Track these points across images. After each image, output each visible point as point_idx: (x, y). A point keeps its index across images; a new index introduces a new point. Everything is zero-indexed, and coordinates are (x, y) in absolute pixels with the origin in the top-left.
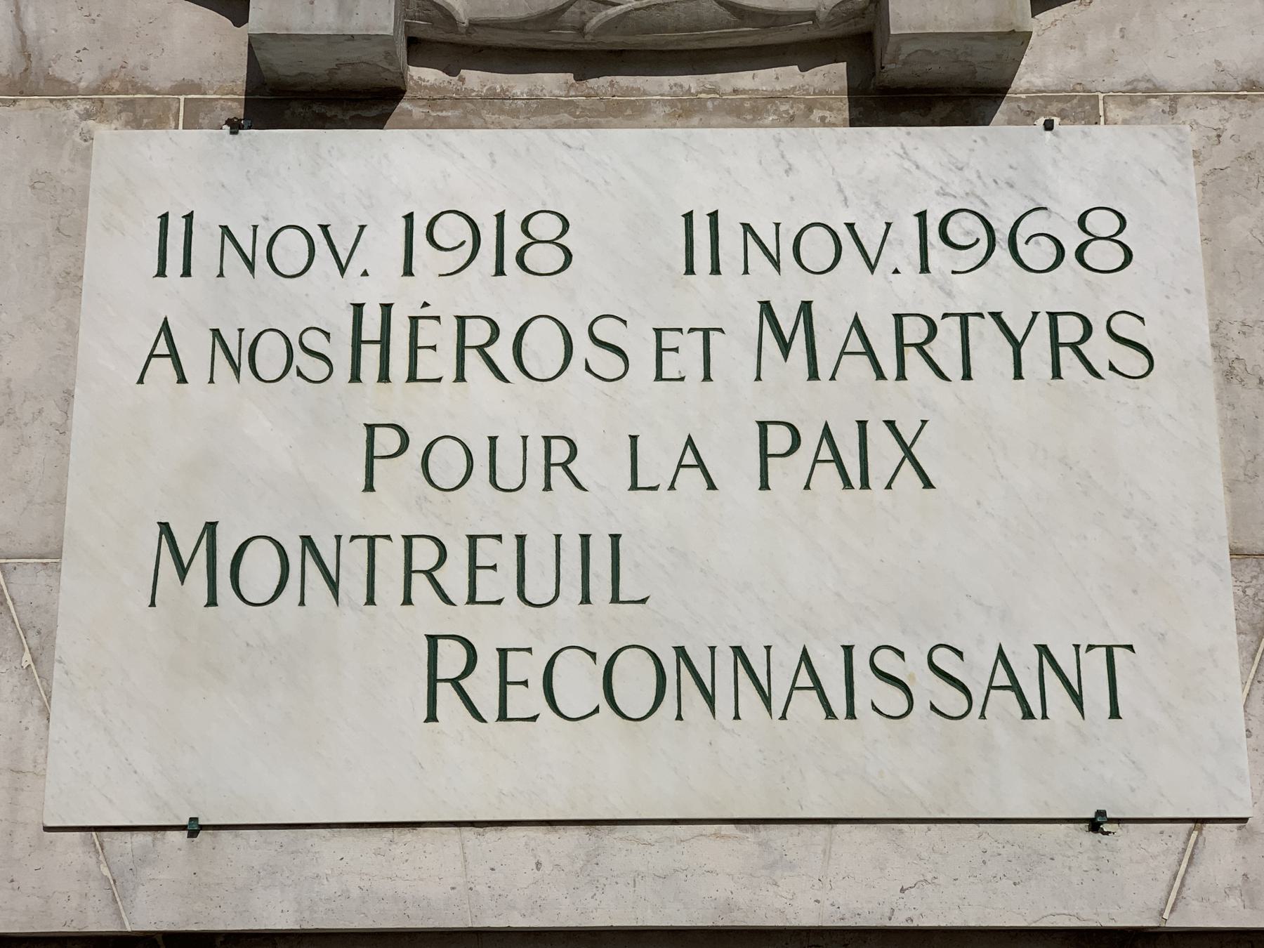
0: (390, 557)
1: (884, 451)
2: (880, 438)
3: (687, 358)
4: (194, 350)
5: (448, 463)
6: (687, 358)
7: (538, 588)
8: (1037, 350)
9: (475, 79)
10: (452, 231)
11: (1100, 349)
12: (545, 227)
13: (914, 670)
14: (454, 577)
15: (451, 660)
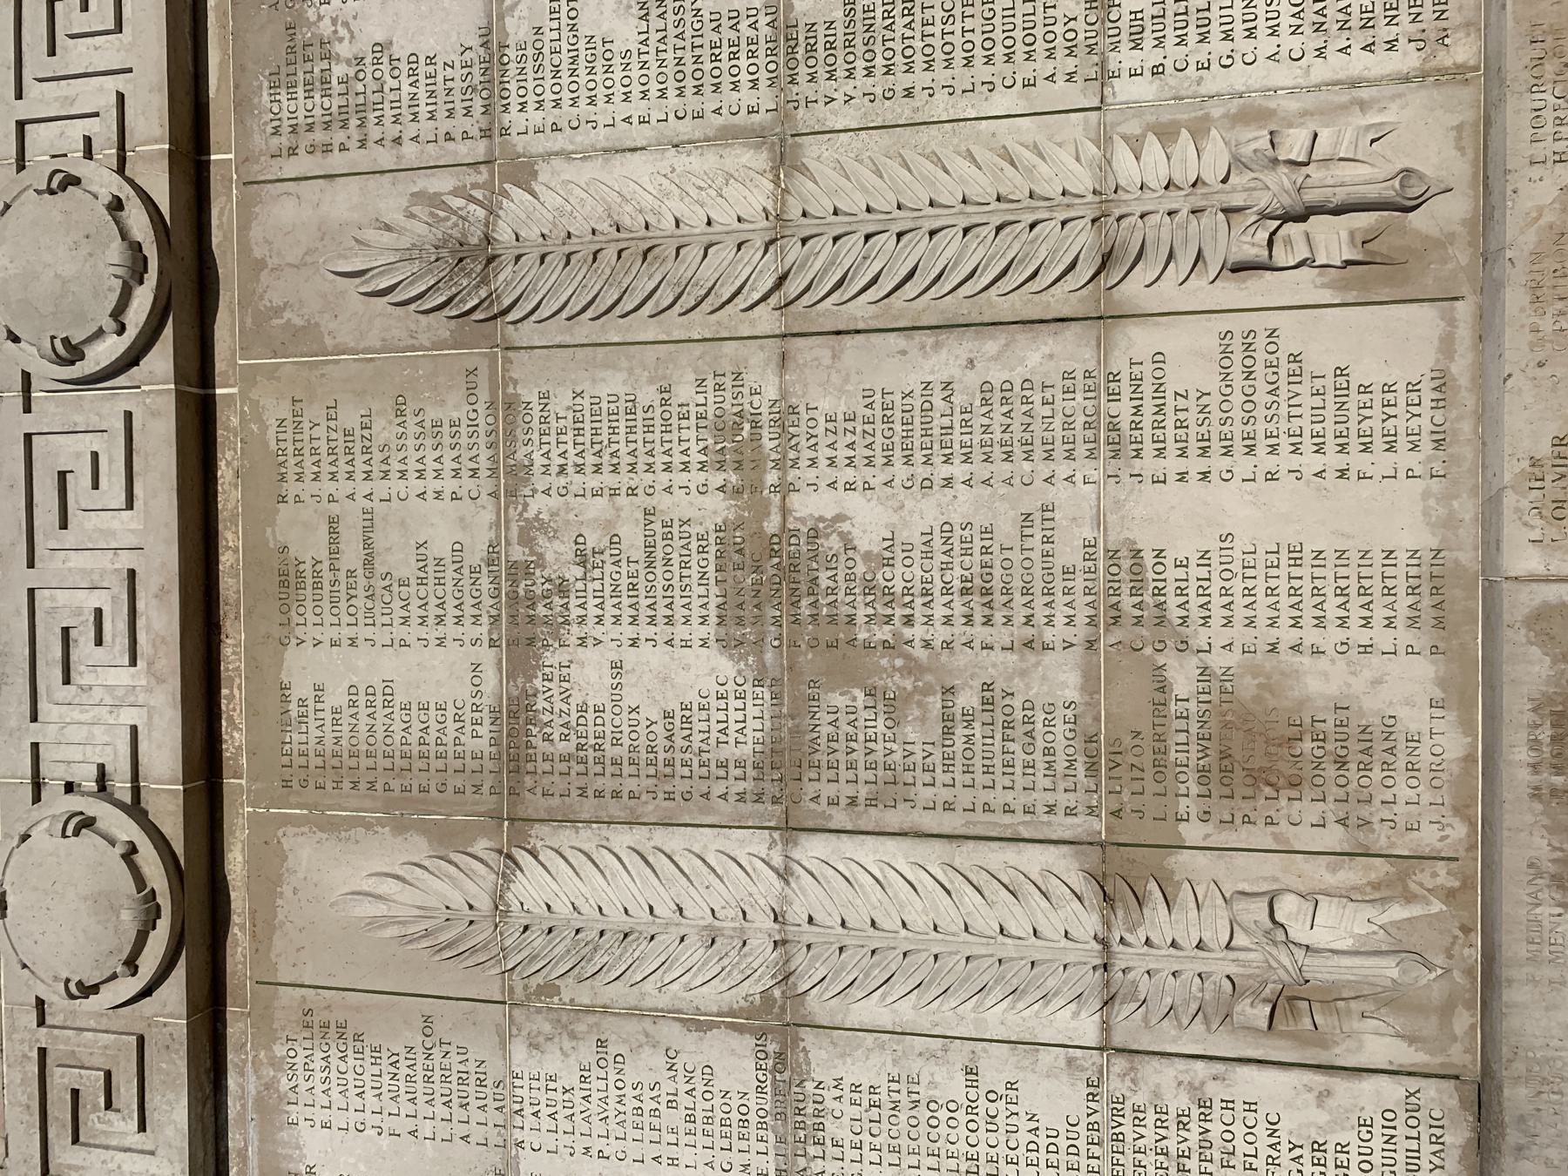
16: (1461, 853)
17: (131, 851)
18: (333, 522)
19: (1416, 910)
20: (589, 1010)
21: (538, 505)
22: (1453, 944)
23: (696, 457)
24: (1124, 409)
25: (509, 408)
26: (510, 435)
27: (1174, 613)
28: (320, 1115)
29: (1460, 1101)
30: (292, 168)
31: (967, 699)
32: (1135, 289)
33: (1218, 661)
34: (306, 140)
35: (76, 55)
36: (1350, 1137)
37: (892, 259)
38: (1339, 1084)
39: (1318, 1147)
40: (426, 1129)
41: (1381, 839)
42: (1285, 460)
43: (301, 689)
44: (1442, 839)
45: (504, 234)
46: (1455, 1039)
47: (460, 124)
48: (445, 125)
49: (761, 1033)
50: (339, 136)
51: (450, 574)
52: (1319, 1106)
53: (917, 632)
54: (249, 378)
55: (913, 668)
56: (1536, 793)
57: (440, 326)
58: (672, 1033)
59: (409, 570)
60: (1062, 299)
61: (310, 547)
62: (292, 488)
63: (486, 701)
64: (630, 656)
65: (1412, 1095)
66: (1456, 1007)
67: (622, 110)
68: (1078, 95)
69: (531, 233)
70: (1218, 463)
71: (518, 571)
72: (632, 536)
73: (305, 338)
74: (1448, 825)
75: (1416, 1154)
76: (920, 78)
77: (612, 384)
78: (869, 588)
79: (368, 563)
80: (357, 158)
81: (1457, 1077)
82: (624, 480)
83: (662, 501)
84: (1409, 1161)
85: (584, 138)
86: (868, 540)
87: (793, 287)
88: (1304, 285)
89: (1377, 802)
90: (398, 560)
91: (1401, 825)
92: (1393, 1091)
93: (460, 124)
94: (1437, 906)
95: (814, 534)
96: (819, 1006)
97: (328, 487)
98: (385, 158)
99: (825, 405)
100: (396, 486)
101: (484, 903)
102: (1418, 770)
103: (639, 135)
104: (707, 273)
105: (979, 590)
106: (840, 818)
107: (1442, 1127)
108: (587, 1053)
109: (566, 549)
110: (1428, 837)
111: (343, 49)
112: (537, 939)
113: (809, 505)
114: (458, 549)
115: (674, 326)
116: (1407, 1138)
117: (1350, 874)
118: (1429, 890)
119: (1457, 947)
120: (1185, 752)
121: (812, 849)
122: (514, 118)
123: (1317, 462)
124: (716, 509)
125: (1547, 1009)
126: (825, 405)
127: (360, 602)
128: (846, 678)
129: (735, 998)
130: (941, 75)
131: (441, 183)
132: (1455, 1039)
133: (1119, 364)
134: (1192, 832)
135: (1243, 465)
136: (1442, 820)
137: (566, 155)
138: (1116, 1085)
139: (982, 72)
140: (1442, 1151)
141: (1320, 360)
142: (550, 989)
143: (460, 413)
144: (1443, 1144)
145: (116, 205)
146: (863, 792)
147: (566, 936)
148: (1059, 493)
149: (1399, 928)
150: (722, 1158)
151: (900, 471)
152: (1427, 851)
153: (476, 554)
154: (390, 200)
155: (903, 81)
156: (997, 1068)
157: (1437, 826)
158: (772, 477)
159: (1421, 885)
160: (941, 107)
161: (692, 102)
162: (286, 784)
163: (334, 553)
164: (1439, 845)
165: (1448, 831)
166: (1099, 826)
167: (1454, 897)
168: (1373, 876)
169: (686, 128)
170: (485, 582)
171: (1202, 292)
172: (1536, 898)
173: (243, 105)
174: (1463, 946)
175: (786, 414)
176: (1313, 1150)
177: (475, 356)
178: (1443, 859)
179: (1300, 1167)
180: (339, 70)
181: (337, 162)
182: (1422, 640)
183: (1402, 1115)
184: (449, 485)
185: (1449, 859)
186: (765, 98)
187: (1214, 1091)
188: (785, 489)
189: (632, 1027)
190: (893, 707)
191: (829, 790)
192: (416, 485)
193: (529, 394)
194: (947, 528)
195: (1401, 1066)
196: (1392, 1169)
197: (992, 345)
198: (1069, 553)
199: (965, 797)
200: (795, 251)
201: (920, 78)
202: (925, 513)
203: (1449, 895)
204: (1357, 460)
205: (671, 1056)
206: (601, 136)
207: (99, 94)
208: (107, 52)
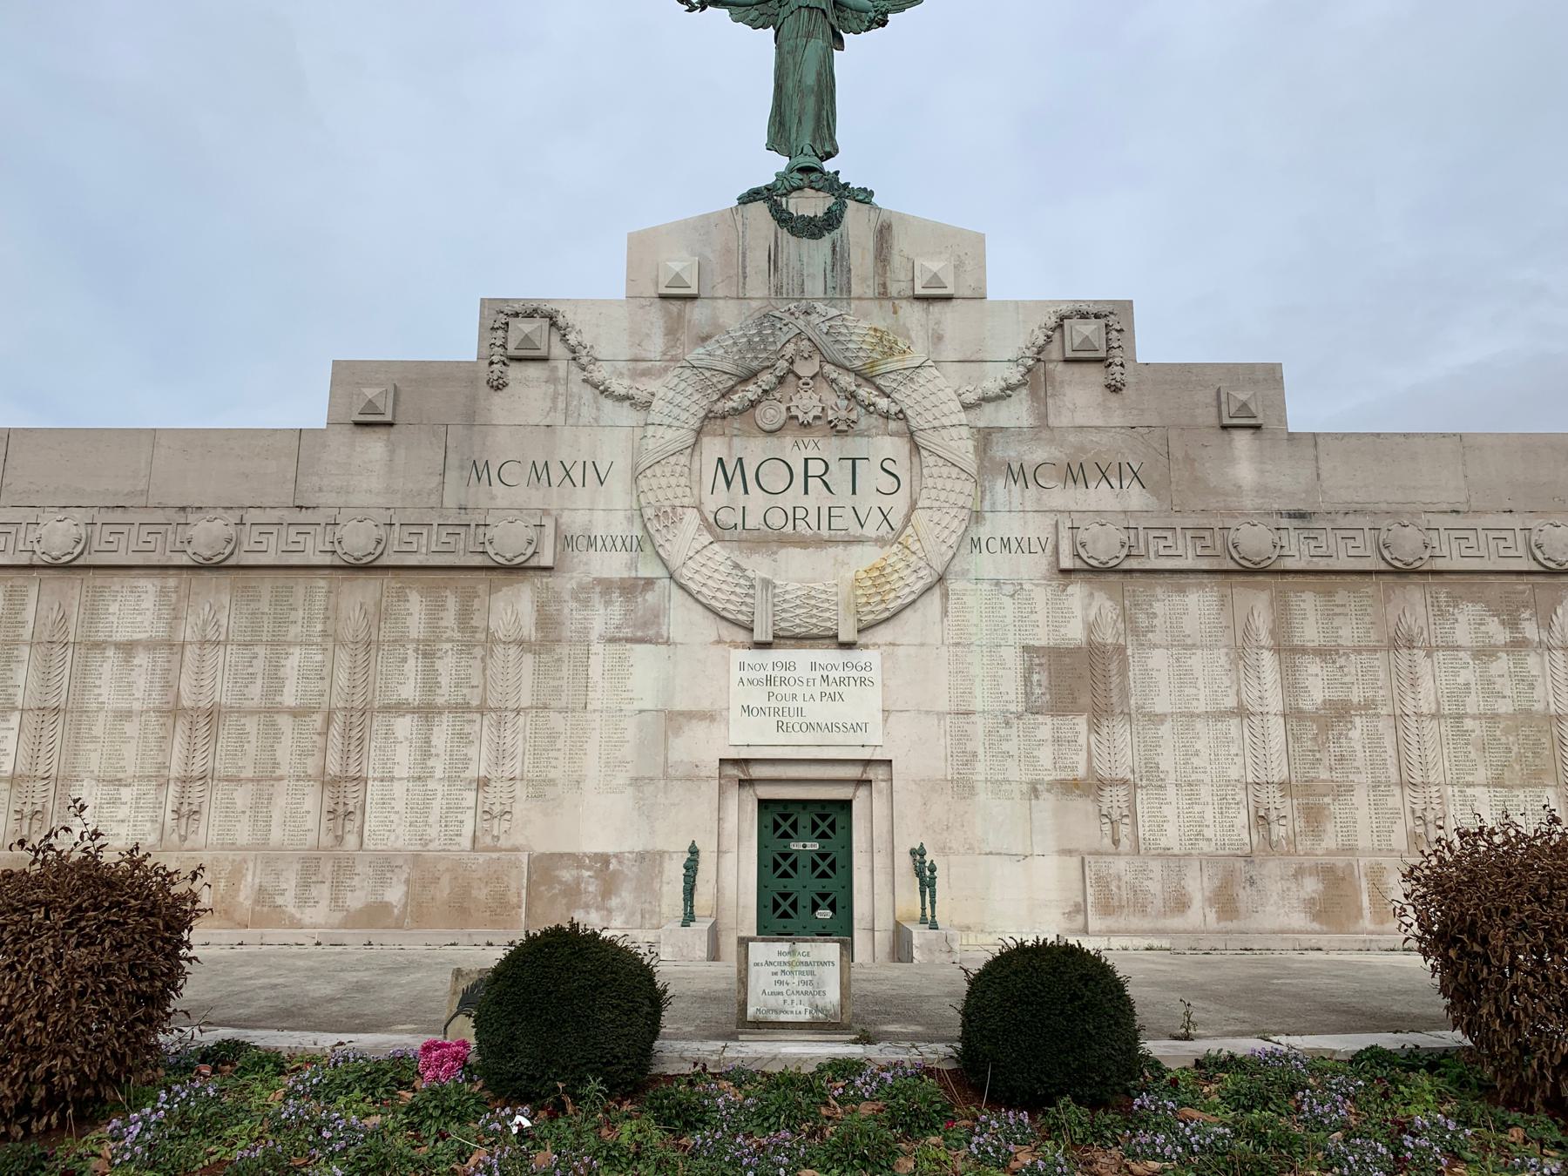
0: (772, 710)
1: (837, 696)
2: (837, 695)
3: (811, 683)
4: (745, 681)
5: (779, 697)
6: (811, 683)
7: (791, 714)
8: (858, 682)
9: (782, 642)
10: (779, 664)
11: (867, 682)
12: (792, 664)
13: (840, 726)
14: (780, 713)
15: (780, 724)
17: (1269, 558)
18: (1345, 605)
20: (1237, 667)
21: (1353, 657)
23: (1367, 695)
24: (1382, 788)
25: (1375, 650)
26: (1369, 650)
27: (1341, 798)
28: (1201, 599)
30: (1428, 596)
31: (1318, 755)
32: (1407, 791)
33: (1332, 807)
34: (1434, 600)
35: (1455, 545)
36: (1236, 832)
37: (1413, 739)
38: (1247, 830)
40: (1203, 626)
41: (1298, 838)
42: (1374, 821)
43: (1304, 596)
45: (1415, 651)
47: (1439, 639)
48: (1439, 636)
49: (1238, 708)
50: (1436, 609)
51: (1334, 635)
53: (1332, 745)
54: (1378, 584)
55: (1323, 744)
57: (1392, 634)
58: (1235, 688)
59: (1334, 625)
60: (1405, 775)
61: (1339, 599)
62: (1352, 595)
63: (1306, 644)
64: (1320, 678)
67: (1443, 678)
68: (1448, 779)
69: (1416, 658)
70: (1373, 807)
71: (1337, 652)
72: (1346, 680)
73: (1388, 600)
76: (1451, 746)
77: (1382, 675)
78: (1341, 734)
79: (1335, 614)
80: (1431, 614)
82: (1360, 678)
83: (1356, 686)
85: (1437, 670)
86: (1350, 734)
87: (1406, 718)
88: (1410, 824)
90: (1338, 621)
92: (1247, 840)
93: (1439, 639)
95: (1351, 722)
96: (1246, 721)
97: (1353, 604)
98: (1431, 621)
99: (1380, 724)
100: (1354, 623)
101: (1263, 644)
103: (1438, 683)
104: (1408, 698)
105: (1342, 758)
106: (1288, 727)
108: (1227, 667)
109: (1343, 664)
110: (1299, 847)
111: (1456, 611)
112: (1256, 656)
113: (1357, 720)
114: (1341, 637)
115: (1396, 691)
117: (1290, 833)
120: (1312, 800)
121: (1281, 721)
122: (1440, 653)
123: (1374, 825)
124: (1355, 700)
126: (1380, 724)
127: (1326, 612)
128: (1318, 728)
129: (1245, 703)
130: (1452, 750)
131: (1425, 634)
133: (1392, 787)
134: (1295, 801)
135: (1373, 812)
137: (1433, 665)
138: (1239, 785)
139: (1453, 759)
141: (1395, 827)
142: (1241, 658)
143: (1372, 638)
145: (1421, 558)
146: (1295, 732)
147: (1256, 663)
148: (1364, 775)
150: (1208, 698)
151: (1367, 741)
153: (1340, 641)
154: (1422, 622)
155: (1451, 742)
156: (1239, 760)
158: (1363, 712)
160: (1445, 751)
161: (1445, 695)
162: (1281, 592)
163: (1337, 606)
166: (1293, 782)
169: (1440, 694)
170: (1333, 644)
171: (1408, 805)
173: (1442, 584)
175: (1377, 715)
177: (1386, 641)
180: (1451, 609)
181: (1430, 608)
182: (1339, 847)
184: (1356, 635)
186: (1446, 712)
187: (1241, 806)
188: (1361, 715)
189: (1234, 678)
190: (1315, 739)
191: (1294, 724)
192: (1355, 626)
193: (1378, 655)
194: (1355, 751)
197: (1395, 761)
198: (1351, 777)
199: (1296, 754)
200: (1414, 718)
201: (1451, 746)
202: (1358, 747)
203: (1289, 851)
204: (1375, 834)
205: (1230, 687)
206: (1437, 674)
207: (1445, 552)
208: (1455, 553)
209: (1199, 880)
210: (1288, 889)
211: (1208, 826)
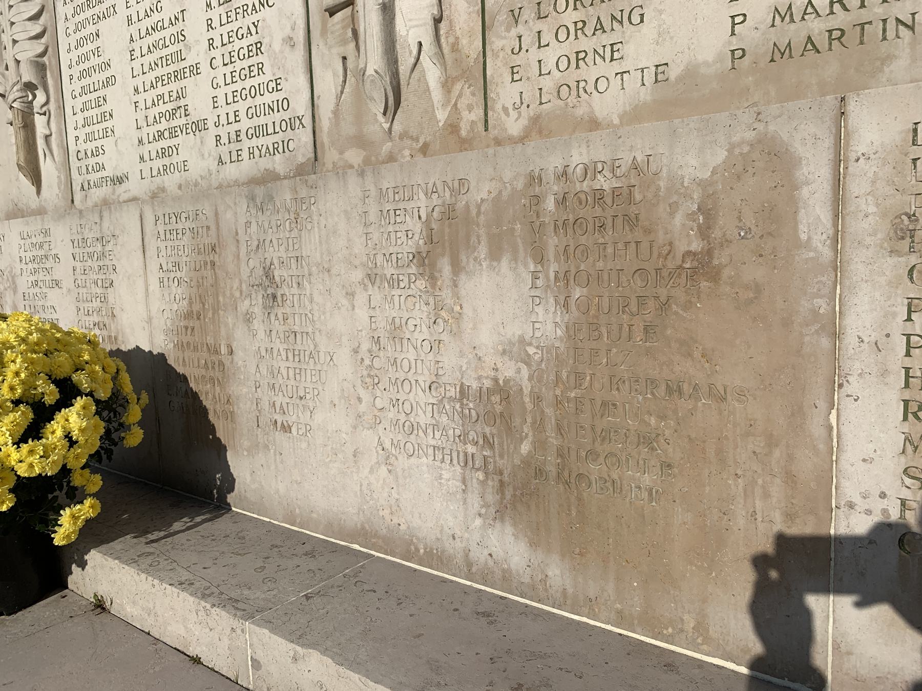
16: (493, 132)
19: (437, 94)
22: (412, 138)
29: (302, 164)
38: (299, 53)
39: (258, 45)
41: (501, 41)
44: (505, 110)
46: (341, 153)
52: (283, 40)
56: (534, 179)
65: (300, 120)
66: (365, 150)
74: (520, 113)
75: (265, 134)
81: (316, 160)
84: (261, 127)
89: (540, 25)
91: (517, 60)
92: (301, 106)
94: (442, 116)
102: (577, 67)
107: (284, 152)
116: (274, 123)
118: (456, 104)
119: (409, 142)
125: (346, 212)
132: (341, 153)
136: (525, 105)
140: (270, 155)
144: (274, 154)
149: (419, 80)
152: (492, 95)
157: (518, 102)
159: (460, 96)
164: (499, 107)
165: (513, 114)
167: (452, 133)
168: (464, 42)
172: (433, 192)
174: (411, 149)
176: (256, 44)
178: (486, 115)
179: (245, 36)
183: (286, 116)
185: (486, 121)
195: (318, 106)
196: (254, 115)
209: (140, 283)
210: (396, 332)
211: (195, 70)
